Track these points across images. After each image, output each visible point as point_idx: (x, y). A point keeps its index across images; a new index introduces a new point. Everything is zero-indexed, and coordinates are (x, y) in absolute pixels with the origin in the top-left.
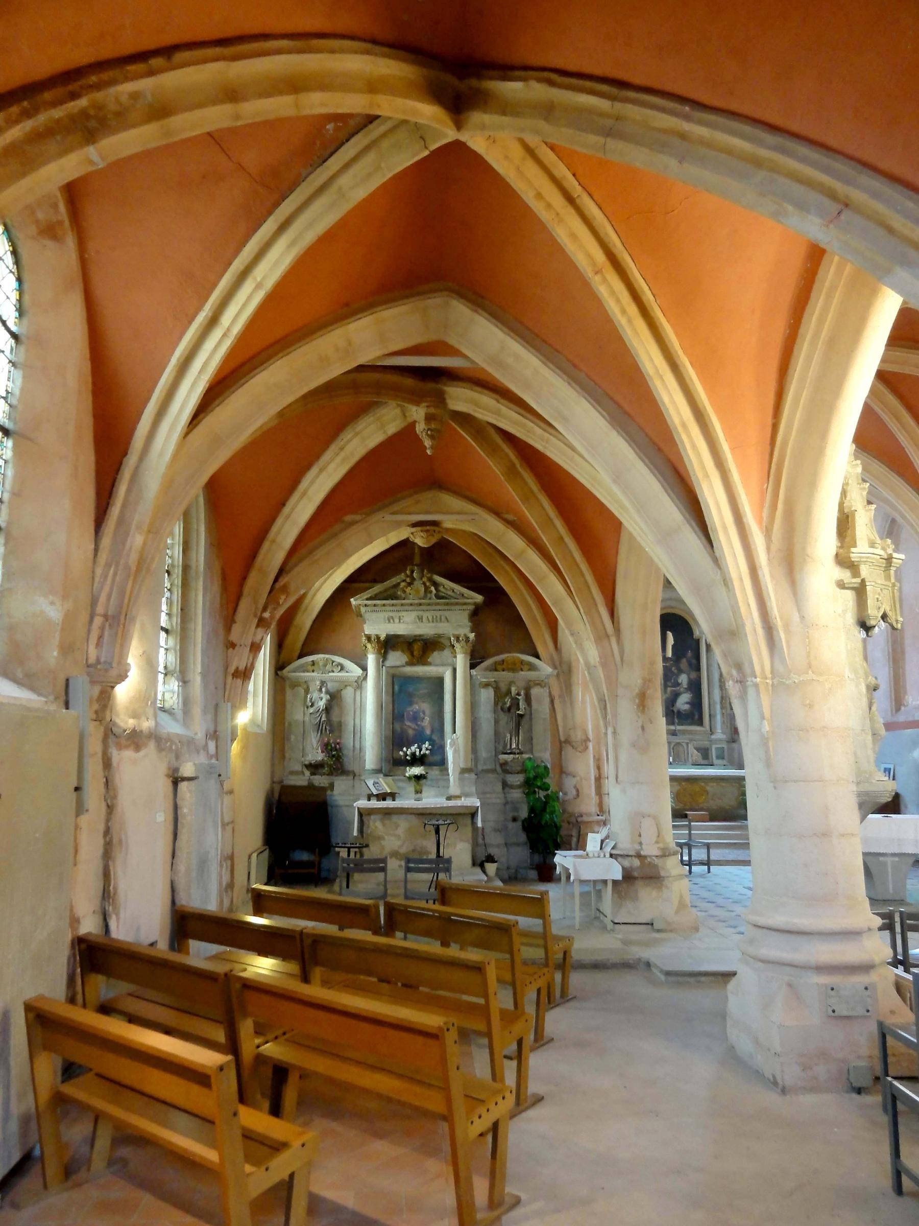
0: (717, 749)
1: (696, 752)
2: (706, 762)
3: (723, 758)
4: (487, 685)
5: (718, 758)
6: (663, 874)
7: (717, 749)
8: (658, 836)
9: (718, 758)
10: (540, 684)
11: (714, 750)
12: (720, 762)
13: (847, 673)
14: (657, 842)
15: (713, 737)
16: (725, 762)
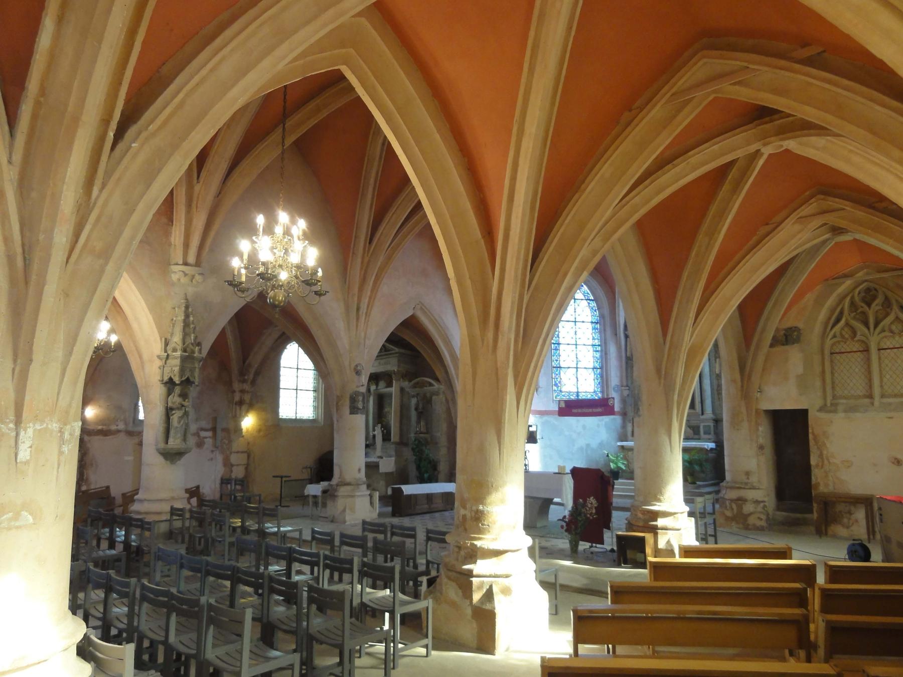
0: (704, 426)
1: (688, 429)
2: (696, 437)
3: (710, 434)
4: (413, 396)
5: (705, 433)
6: (336, 494)
7: (704, 426)
8: (341, 475)
9: (705, 433)
10: (437, 393)
11: (701, 428)
12: (707, 436)
13: (159, 404)
14: (339, 478)
15: (702, 417)
16: (710, 437)
